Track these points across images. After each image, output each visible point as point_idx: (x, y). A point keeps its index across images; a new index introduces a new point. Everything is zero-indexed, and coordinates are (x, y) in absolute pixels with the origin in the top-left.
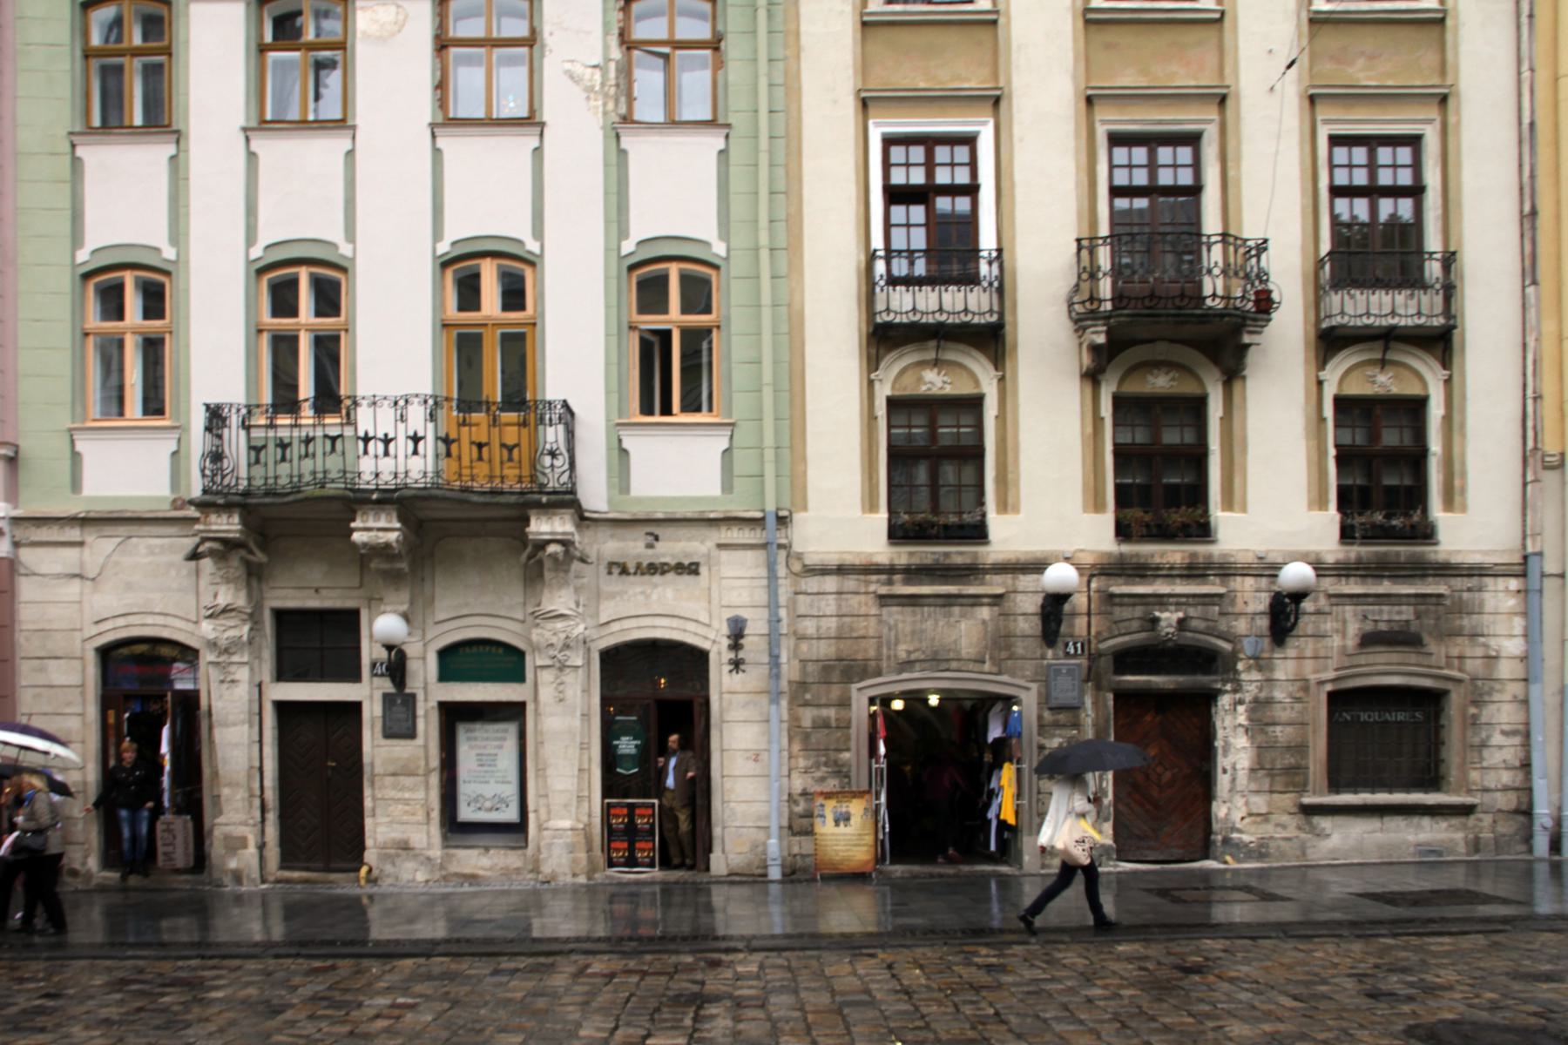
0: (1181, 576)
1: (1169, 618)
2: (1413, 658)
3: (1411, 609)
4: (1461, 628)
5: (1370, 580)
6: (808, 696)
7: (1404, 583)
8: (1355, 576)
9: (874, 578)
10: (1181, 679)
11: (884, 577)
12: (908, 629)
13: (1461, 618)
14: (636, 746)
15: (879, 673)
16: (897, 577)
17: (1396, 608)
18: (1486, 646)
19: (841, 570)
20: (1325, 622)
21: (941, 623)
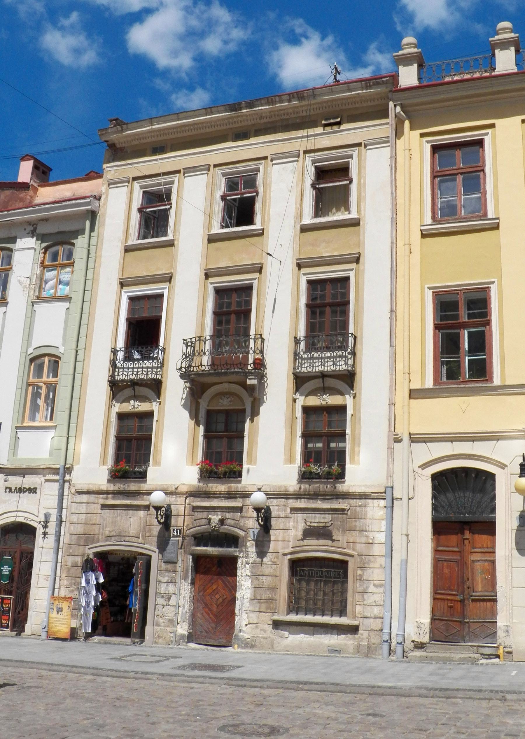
0: (225, 498)
1: (215, 518)
2: (329, 542)
3: (330, 516)
4: (355, 525)
5: (311, 501)
6: (71, 551)
7: (328, 503)
8: (304, 498)
9: (101, 496)
10: (220, 549)
11: (105, 496)
12: (111, 521)
13: (356, 521)
14: (9, 570)
15: (98, 541)
16: (110, 496)
17: (323, 515)
18: (367, 537)
19: (89, 492)
20: (289, 522)
21: (123, 518)
